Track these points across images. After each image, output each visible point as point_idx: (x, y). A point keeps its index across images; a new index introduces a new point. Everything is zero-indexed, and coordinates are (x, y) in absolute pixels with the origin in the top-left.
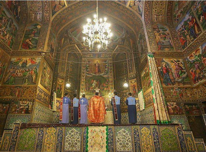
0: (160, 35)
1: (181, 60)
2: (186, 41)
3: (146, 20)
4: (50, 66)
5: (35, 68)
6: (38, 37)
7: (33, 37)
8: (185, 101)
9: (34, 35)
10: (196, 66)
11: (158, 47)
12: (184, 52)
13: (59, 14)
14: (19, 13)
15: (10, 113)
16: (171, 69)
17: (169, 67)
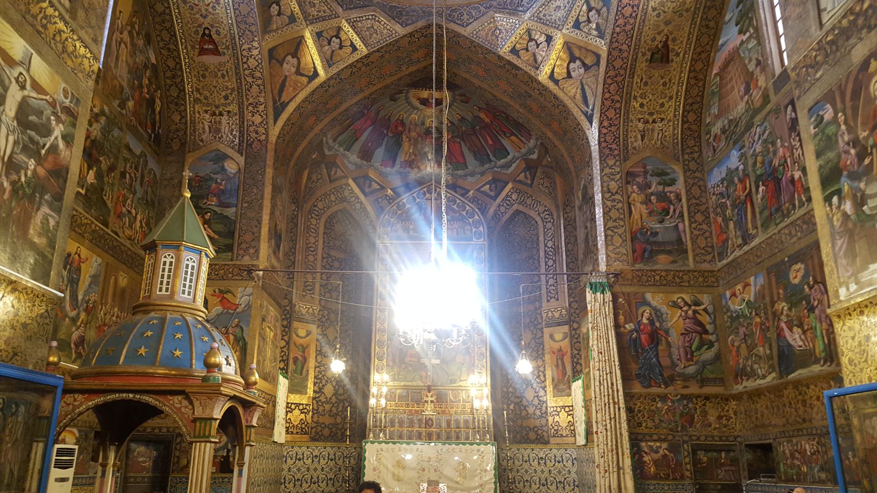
0: (647, 201)
1: (706, 299)
2: (727, 240)
3: (605, 141)
4: (274, 299)
5: (237, 326)
6: (234, 209)
7: (217, 209)
8: (698, 439)
9: (220, 201)
10: (742, 330)
11: (634, 252)
12: (718, 270)
13: (298, 107)
14: (157, 117)
15: (173, 472)
16: (667, 332)
17: (661, 324)
